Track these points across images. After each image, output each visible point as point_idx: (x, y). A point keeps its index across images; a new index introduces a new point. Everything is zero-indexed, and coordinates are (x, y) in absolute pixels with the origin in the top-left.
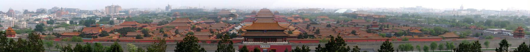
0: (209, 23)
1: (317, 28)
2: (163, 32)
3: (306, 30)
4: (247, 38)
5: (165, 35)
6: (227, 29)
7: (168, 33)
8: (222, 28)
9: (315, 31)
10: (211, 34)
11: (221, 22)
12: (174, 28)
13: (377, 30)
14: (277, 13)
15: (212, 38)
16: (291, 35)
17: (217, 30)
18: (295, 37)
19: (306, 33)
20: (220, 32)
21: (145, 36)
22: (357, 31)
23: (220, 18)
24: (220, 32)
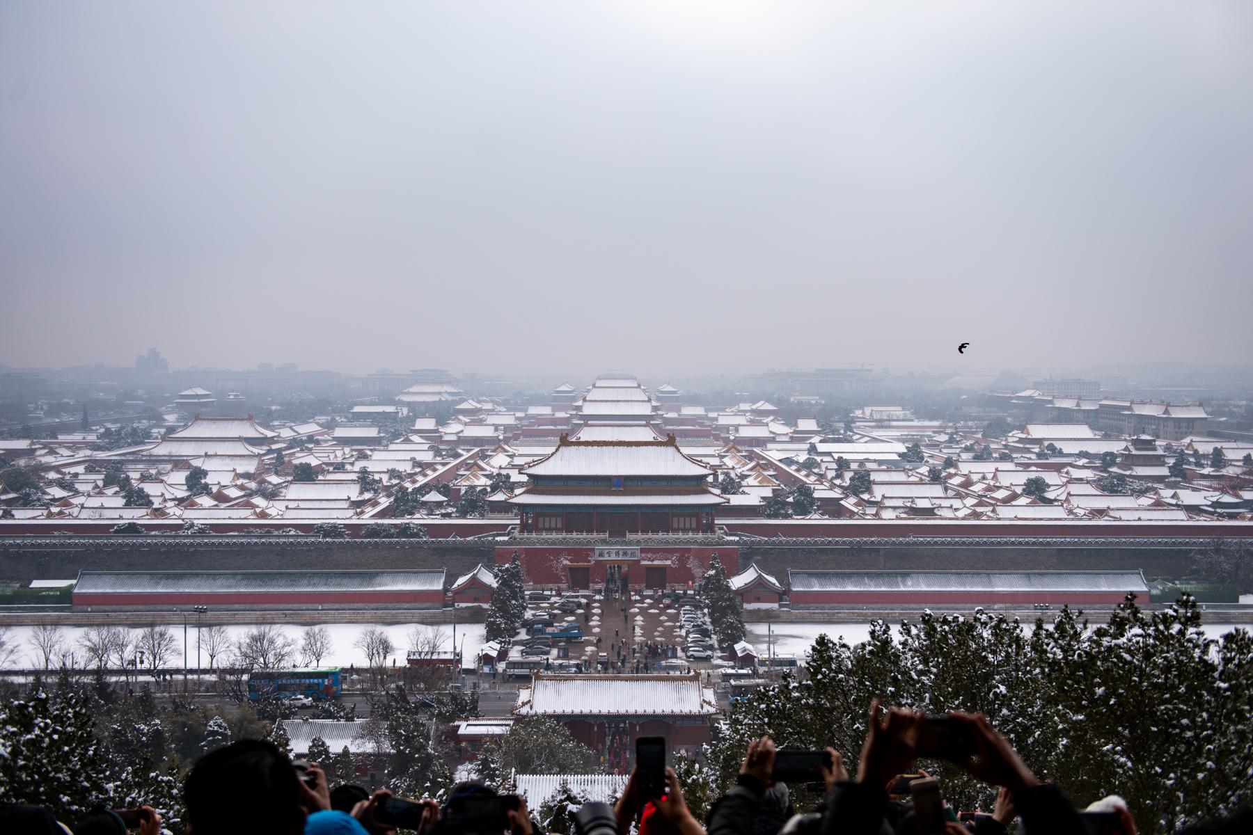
1: (854, 466)
2: (125, 484)
3: (801, 475)
5: (136, 498)
6: (441, 469)
7: (151, 489)
8: (416, 463)
10: (367, 496)
11: (415, 438)
12: (179, 463)
13: (1160, 479)
15: (370, 511)
16: (736, 500)
19: (805, 491)
20: (410, 486)
21: (26, 502)
22: (1051, 478)
23: (412, 420)
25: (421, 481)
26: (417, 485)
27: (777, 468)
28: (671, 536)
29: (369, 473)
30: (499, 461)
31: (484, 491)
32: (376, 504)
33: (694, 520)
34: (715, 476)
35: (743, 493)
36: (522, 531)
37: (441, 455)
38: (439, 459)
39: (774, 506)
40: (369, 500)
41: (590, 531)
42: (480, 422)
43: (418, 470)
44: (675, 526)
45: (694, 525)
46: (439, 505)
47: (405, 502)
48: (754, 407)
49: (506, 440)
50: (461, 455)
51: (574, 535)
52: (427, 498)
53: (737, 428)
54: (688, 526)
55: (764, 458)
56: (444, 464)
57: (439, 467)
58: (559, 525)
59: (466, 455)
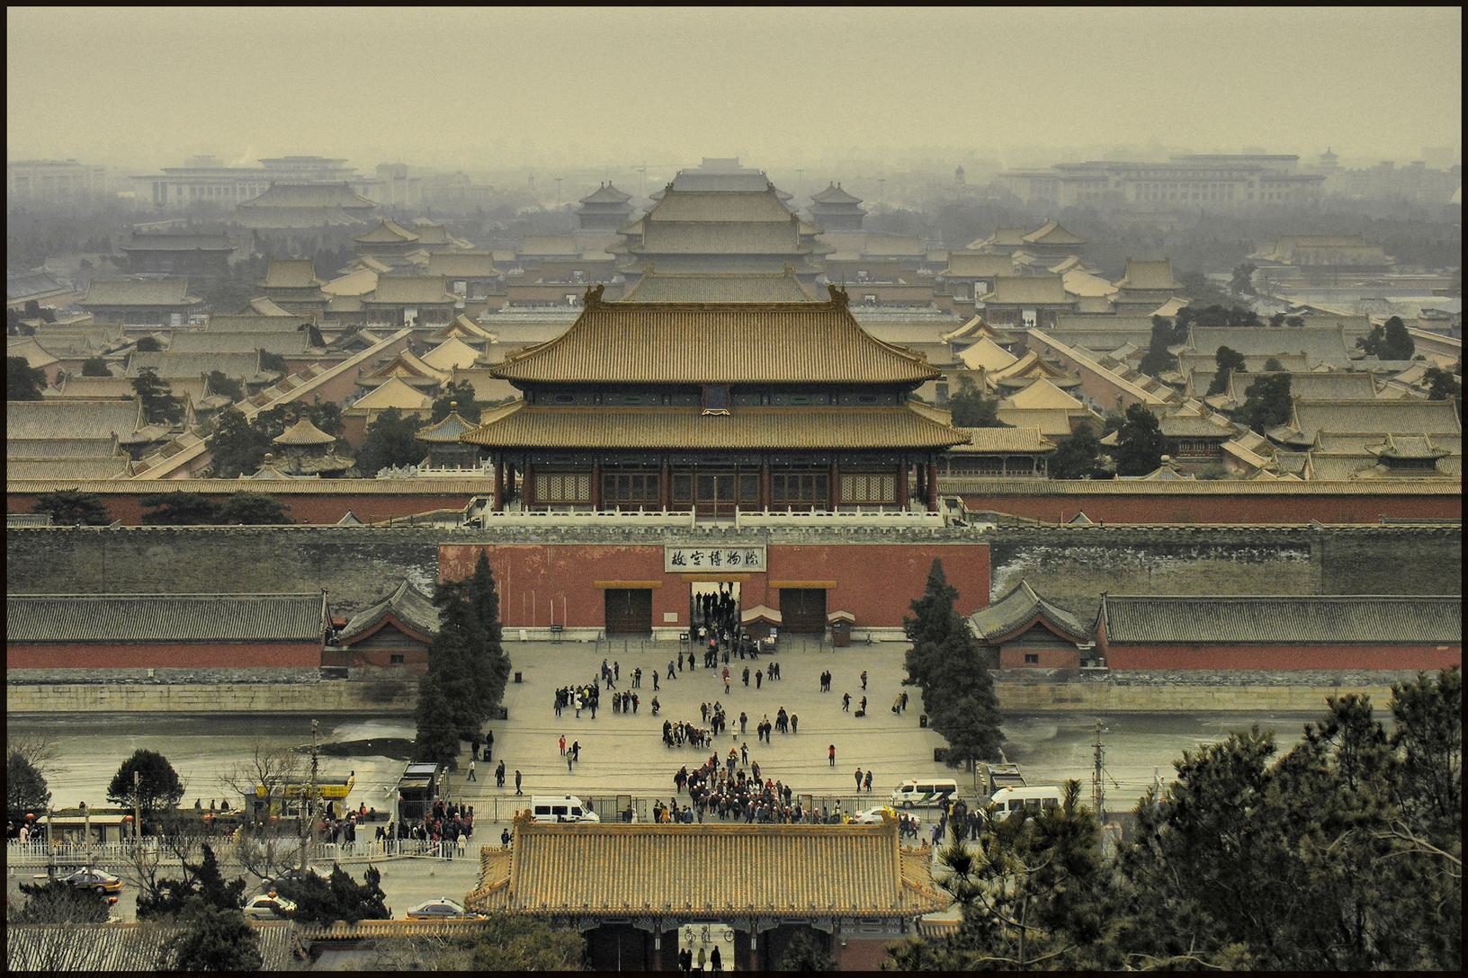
0: (134, 313)
3: (1137, 390)
4: (523, 472)
6: (323, 375)
9: (1236, 396)
14: (839, 208)
16: (984, 440)
17: (218, 384)
18: (1020, 461)
19: (1141, 420)
20: (250, 412)
24: (250, 412)
25: (277, 397)
26: (269, 407)
27: (1081, 371)
28: (837, 518)
29: (156, 381)
30: (453, 356)
31: (414, 422)
32: (166, 447)
33: (890, 482)
34: (942, 389)
35: (1000, 424)
36: (499, 508)
37: (323, 345)
38: (318, 352)
39: (1072, 454)
40: (160, 442)
41: (653, 508)
42: (417, 275)
43: (271, 376)
44: (846, 495)
45: (889, 495)
46: (317, 449)
47: (239, 446)
48: (1031, 238)
49: (472, 310)
50: (370, 344)
51: (617, 518)
52: (290, 435)
53: (991, 283)
54: (875, 496)
55: (1049, 349)
56: (329, 363)
57: (316, 368)
58: (584, 495)
59: (380, 344)
